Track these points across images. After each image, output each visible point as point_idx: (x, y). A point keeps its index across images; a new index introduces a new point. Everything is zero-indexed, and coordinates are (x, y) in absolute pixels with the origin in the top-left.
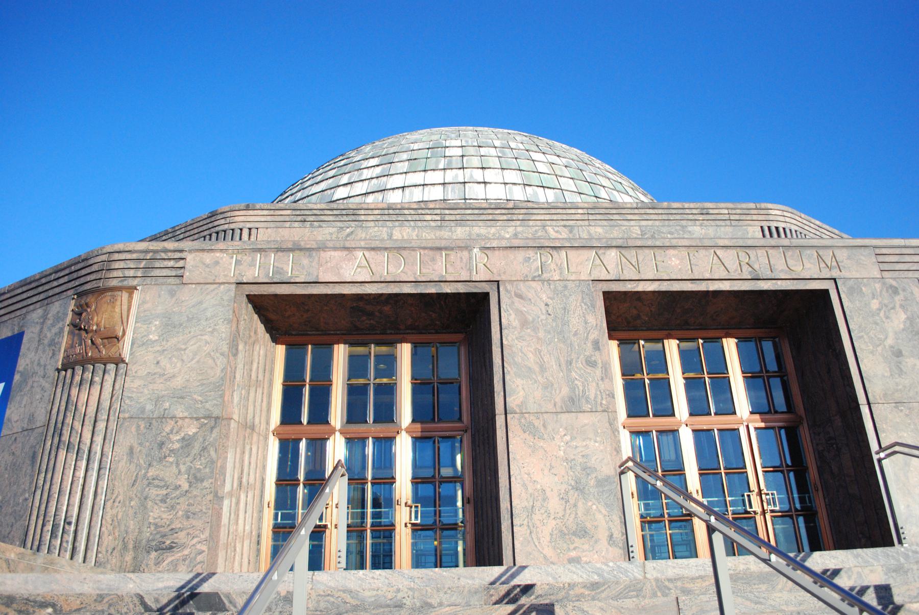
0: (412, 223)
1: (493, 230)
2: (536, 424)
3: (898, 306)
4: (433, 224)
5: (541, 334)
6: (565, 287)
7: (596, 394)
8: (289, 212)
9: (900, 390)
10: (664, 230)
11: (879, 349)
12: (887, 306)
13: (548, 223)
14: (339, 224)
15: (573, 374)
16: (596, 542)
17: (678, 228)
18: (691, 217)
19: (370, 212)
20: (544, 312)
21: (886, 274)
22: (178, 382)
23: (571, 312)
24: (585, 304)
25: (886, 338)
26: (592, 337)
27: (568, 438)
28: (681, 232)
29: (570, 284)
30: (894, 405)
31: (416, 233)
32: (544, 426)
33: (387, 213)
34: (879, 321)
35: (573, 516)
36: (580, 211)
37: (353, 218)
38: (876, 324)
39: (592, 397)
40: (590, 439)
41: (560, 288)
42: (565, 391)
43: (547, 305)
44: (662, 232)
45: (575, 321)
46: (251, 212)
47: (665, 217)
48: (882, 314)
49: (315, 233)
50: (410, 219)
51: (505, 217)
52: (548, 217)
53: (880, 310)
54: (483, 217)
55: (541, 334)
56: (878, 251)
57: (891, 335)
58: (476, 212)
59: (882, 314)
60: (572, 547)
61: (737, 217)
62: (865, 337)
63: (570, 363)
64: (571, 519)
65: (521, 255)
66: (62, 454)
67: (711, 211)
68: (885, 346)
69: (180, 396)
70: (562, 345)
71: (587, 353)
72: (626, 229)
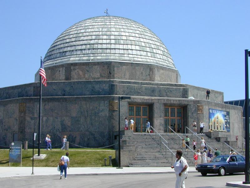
22: (123, 113)
26: (163, 109)
45: (161, 108)
55: (158, 109)
66: (112, 120)
69: (123, 114)
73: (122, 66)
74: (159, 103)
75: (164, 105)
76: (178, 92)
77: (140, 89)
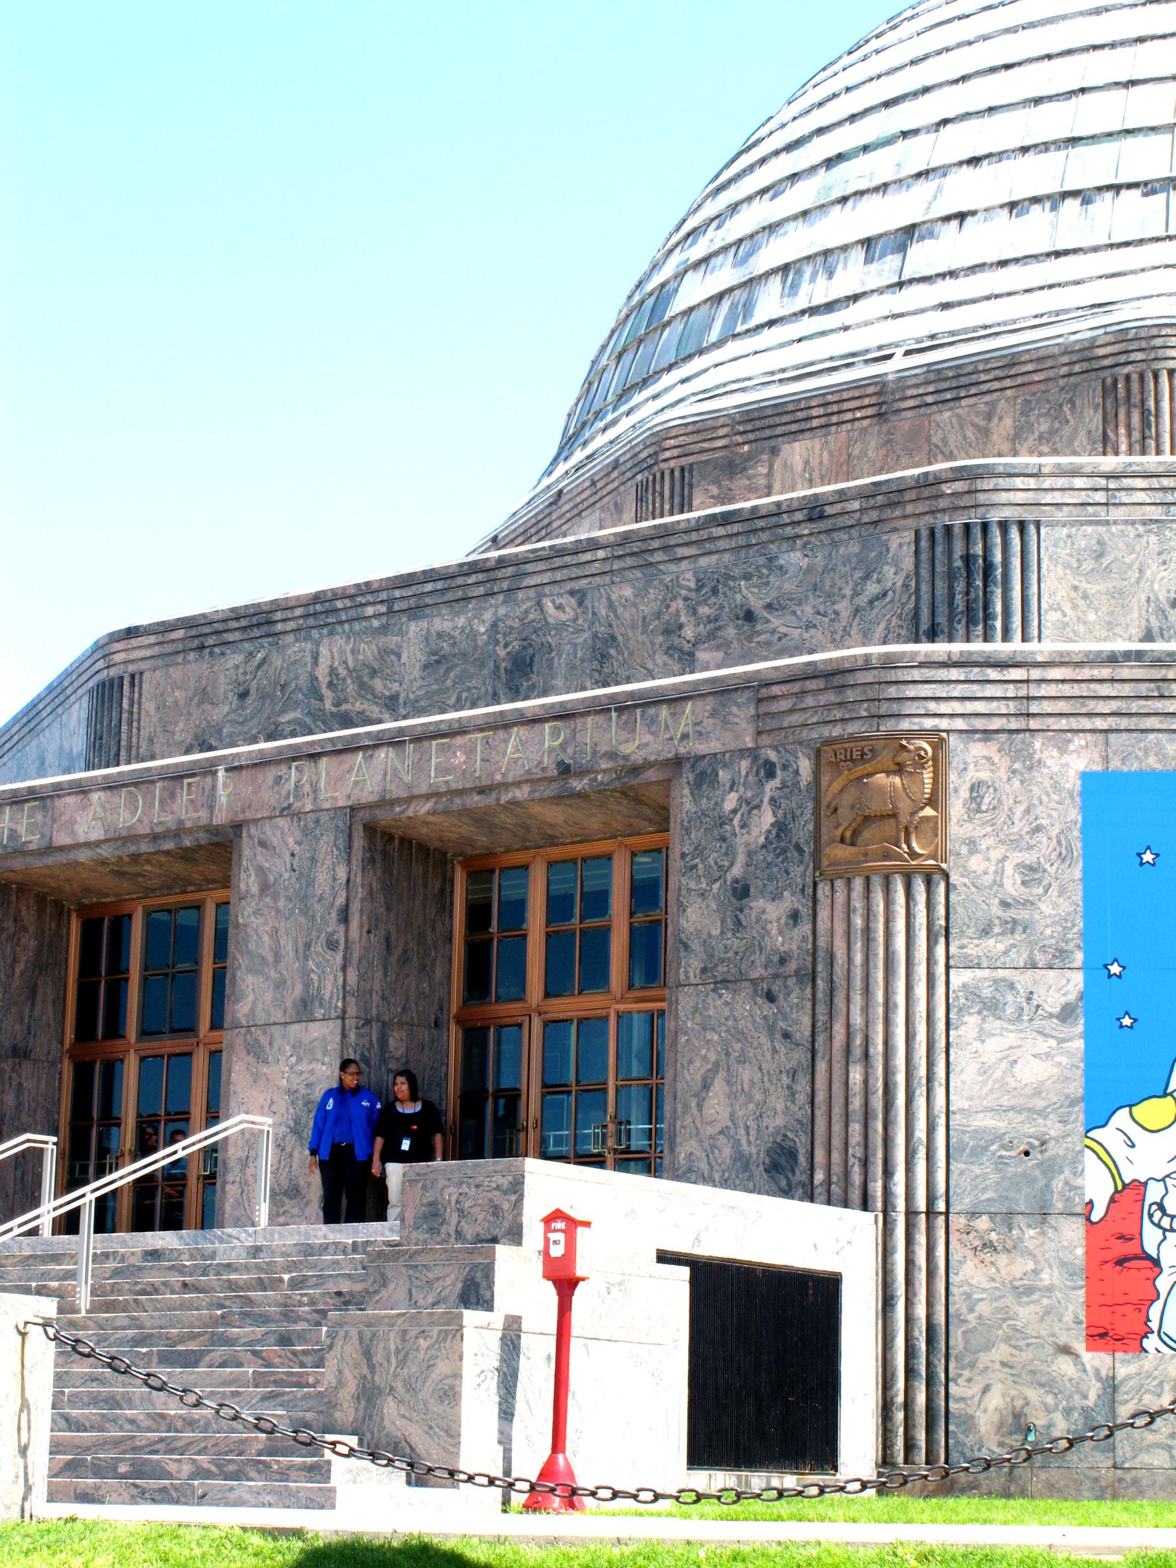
0: (346, 626)
1: (461, 621)
2: (262, 1042)
3: (766, 800)
4: (376, 623)
5: (281, 904)
6: (317, 822)
7: (332, 992)
8: (180, 634)
9: (729, 959)
10: (736, 572)
11: (716, 886)
12: (748, 803)
13: (547, 590)
14: (247, 646)
15: (311, 963)
16: (307, 1204)
17: (762, 561)
18: (789, 531)
19: (289, 614)
20: (288, 866)
21: (766, 740)
23: (319, 864)
24: (338, 849)
25: (732, 865)
27: (293, 1059)
28: (765, 571)
29: (324, 817)
30: (712, 986)
31: (351, 646)
32: (271, 1044)
33: (312, 612)
34: (728, 835)
35: (287, 1169)
36: (601, 554)
37: (266, 629)
38: (724, 839)
39: (327, 997)
40: (318, 1060)
41: (311, 825)
42: (299, 989)
43: (293, 855)
44: (733, 578)
45: (322, 877)
46: (134, 642)
47: (741, 541)
48: (736, 822)
49: (216, 669)
50: (344, 618)
51: (481, 590)
52: (546, 578)
53: (734, 811)
54: (450, 596)
56: (764, 692)
57: (741, 859)
58: (440, 585)
59: (736, 822)
60: (281, 1210)
61: (874, 515)
62: (700, 866)
63: (308, 946)
64: (285, 1174)
65: (271, 773)
67: (829, 510)
68: (725, 881)
70: (303, 920)
71: (330, 929)
72: (672, 580)
73: (774, 451)
74: (298, 815)
75: (359, 843)
76: (844, 607)
77: (374, 673)
